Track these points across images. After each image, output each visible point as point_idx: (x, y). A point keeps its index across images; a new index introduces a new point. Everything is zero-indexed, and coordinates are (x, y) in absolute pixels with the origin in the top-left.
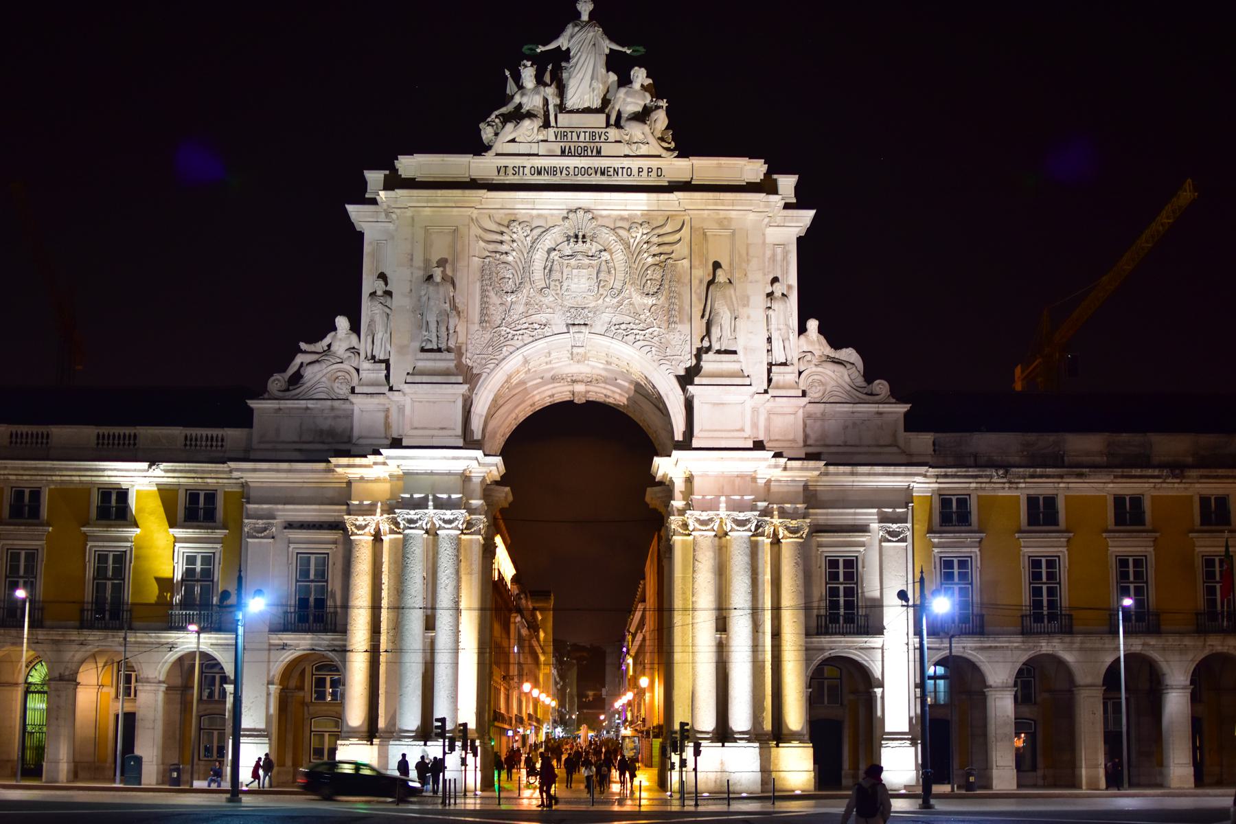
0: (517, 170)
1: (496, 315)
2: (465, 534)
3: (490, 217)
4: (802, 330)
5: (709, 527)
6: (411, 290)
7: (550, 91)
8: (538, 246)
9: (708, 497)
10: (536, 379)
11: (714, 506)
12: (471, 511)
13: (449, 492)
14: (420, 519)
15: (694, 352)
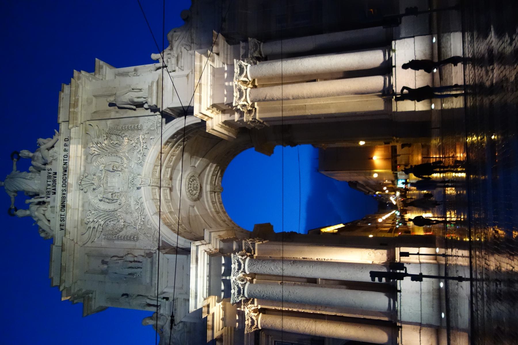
0: (62, 219)
1: (130, 231)
2: (254, 254)
3: (82, 235)
4: (157, 61)
5: (244, 91)
6: (117, 283)
7: (28, 201)
8: (97, 206)
9: (226, 93)
10: (194, 210)
11: (230, 90)
12: (240, 249)
13: (221, 265)
14: (238, 286)
15: (153, 113)
